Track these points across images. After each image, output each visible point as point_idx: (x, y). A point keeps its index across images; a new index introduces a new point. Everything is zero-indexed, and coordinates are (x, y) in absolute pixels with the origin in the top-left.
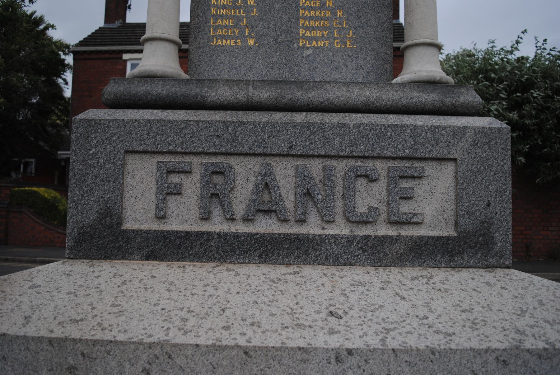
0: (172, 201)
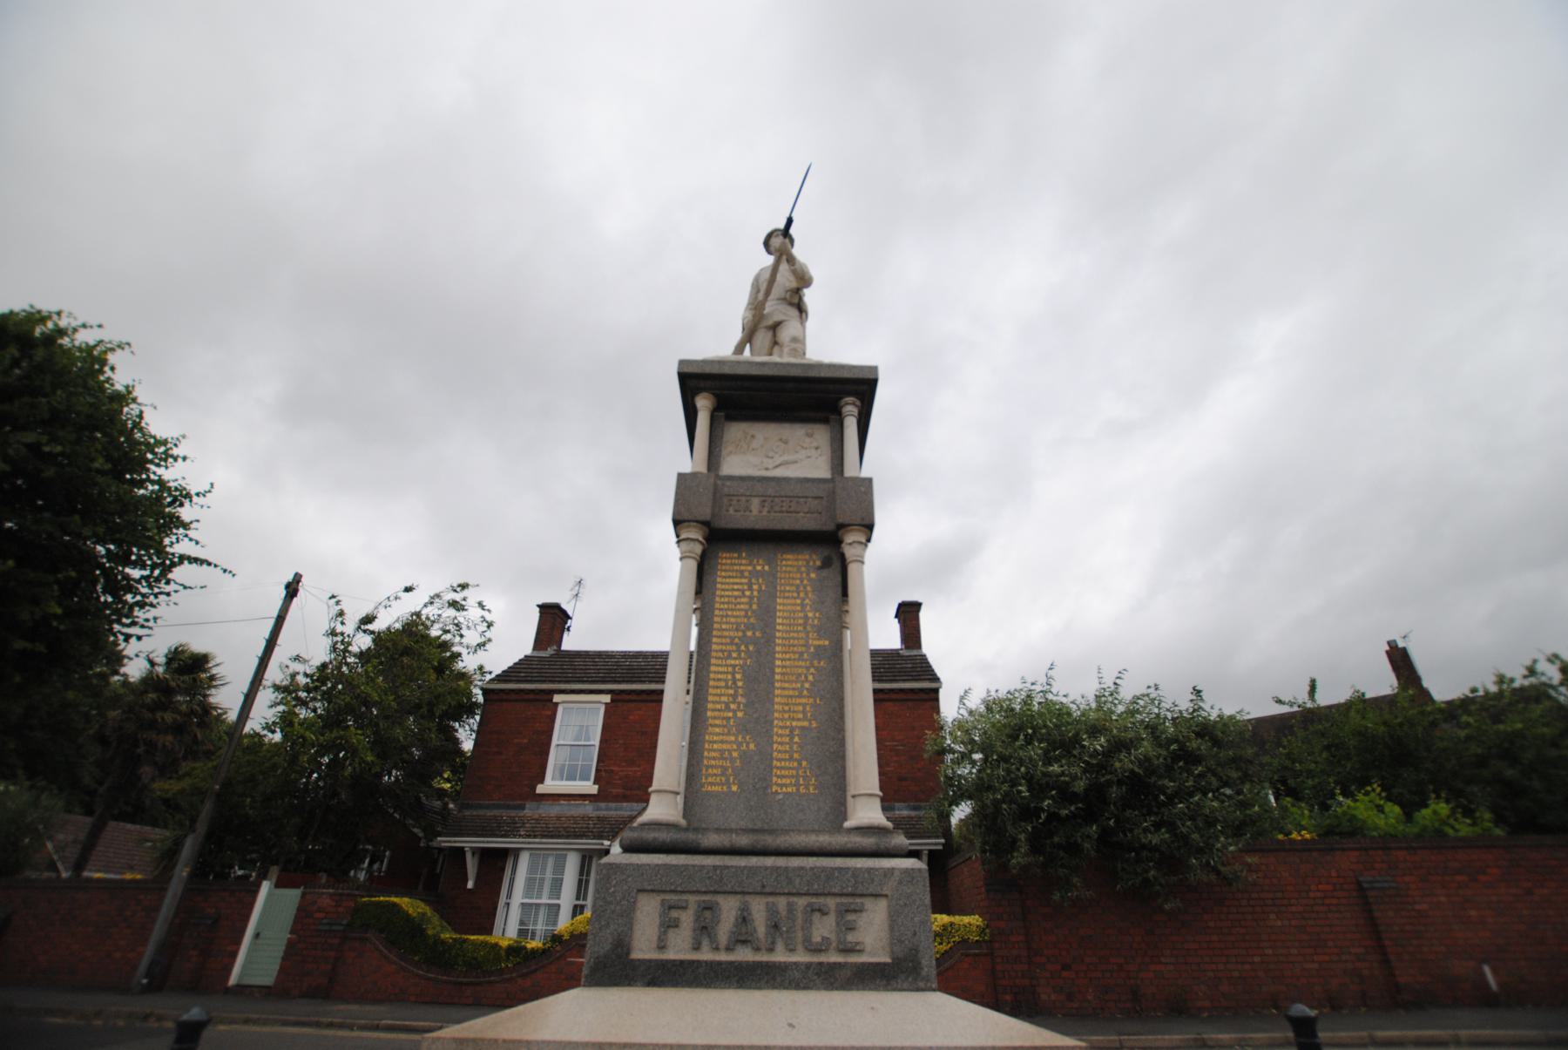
0: (671, 934)
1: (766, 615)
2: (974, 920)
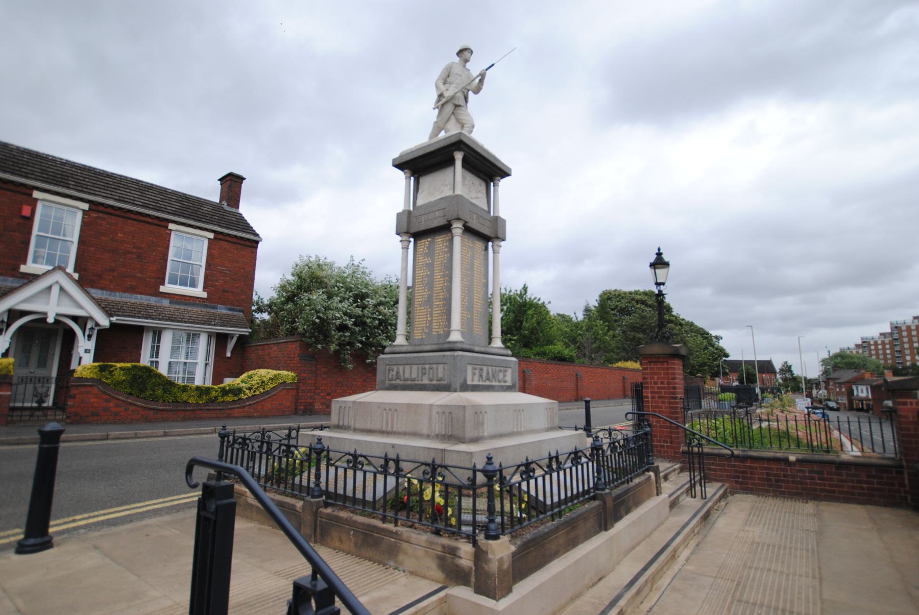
1: (472, 265)
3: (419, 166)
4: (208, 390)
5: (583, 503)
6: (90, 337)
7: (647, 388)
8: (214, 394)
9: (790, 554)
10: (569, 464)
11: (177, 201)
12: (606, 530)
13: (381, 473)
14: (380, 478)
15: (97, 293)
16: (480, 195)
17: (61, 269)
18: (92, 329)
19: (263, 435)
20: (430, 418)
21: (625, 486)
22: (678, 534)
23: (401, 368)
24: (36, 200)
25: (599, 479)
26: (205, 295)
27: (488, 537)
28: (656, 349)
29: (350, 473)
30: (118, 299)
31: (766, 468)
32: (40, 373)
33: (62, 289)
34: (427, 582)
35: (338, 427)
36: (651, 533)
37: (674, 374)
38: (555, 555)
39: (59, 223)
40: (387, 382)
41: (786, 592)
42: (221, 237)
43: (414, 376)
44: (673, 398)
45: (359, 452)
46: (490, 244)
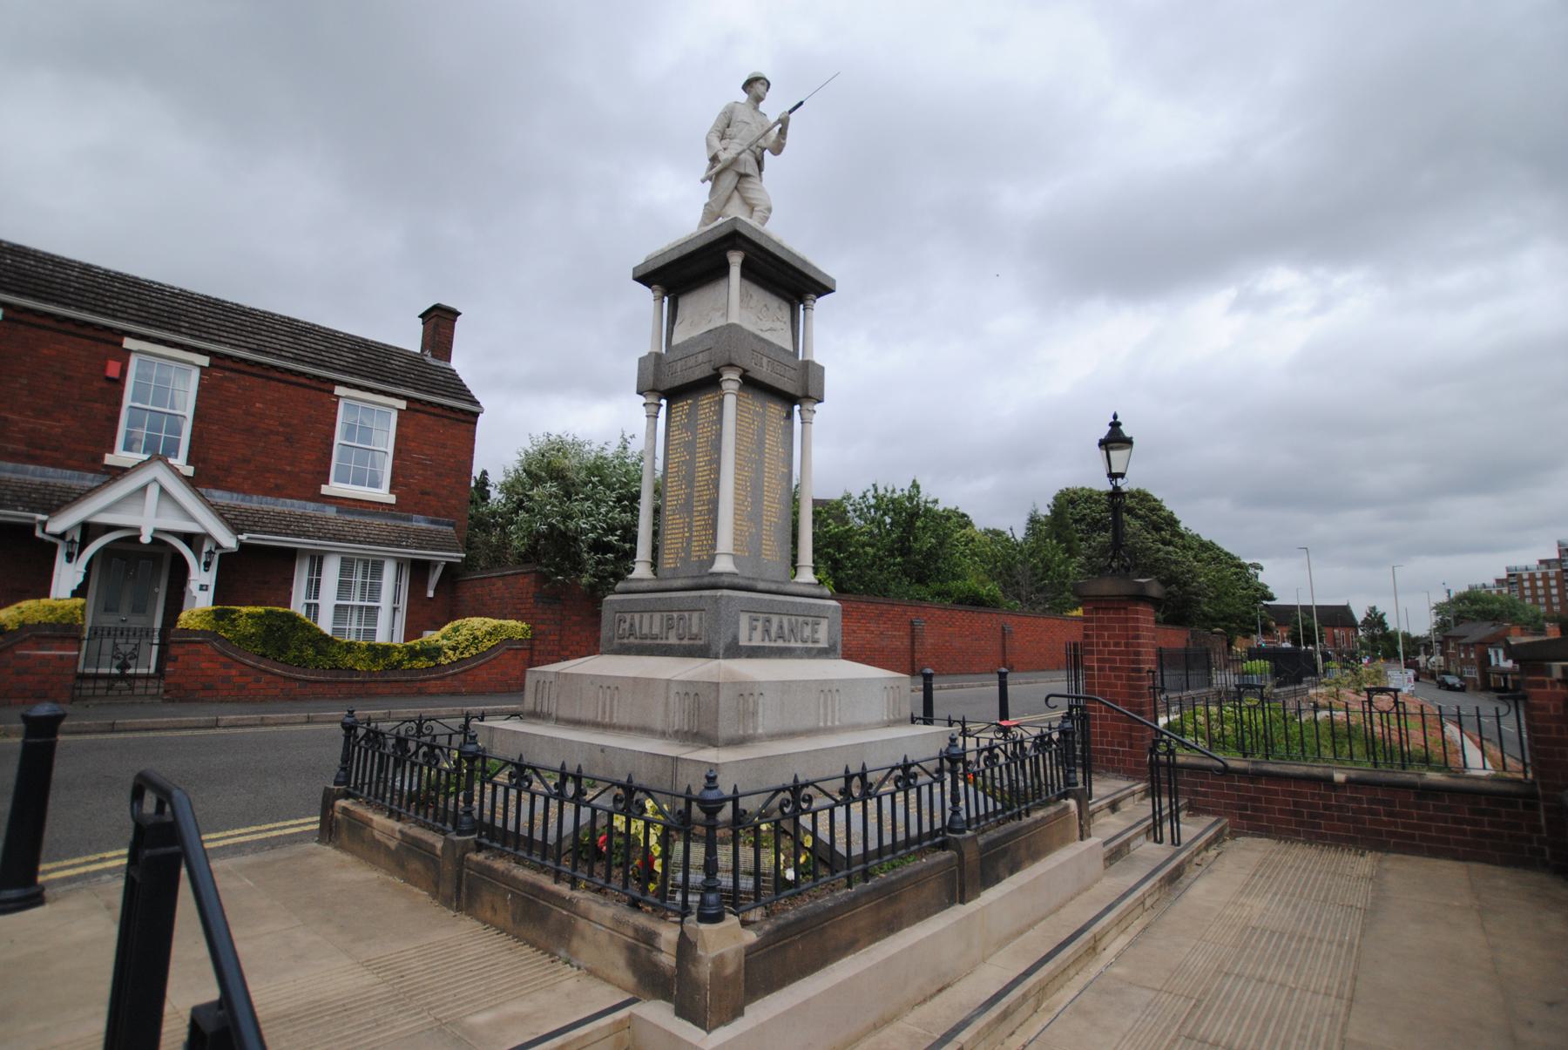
1: (761, 443)
2: (521, 625)
3: (677, 276)
4: (387, 650)
5: (922, 853)
6: (207, 565)
7: (1092, 653)
8: (396, 656)
9: (1307, 950)
10: (889, 787)
11: (352, 351)
12: (962, 902)
13: (556, 796)
14: (554, 803)
15: (221, 497)
16: (778, 325)
17: (163, 459)
18: (210, 553)
19: (420, 726)
20: (667, 704)
21: (1013, 825)
22: (1109, 908)
23: (637, 616)
24: (129, 352)
25: (955, 812)
26: (392, 499)
27: (704, 918)
28: (1107, 587)
29: (513, 793)
30: (255, 506)
31: (1294, 794)
32: (136, 622)
33: (163, 491)
34: (609, 988)
35: (536, 715)
36: (1061, 906)
37: (1137, 628)
38: (850, 946)
39: (164, 386)
40: (616, 641)
41: (1279, 1024)
42: (417, 406)
43: (656, 630)
44: (1134, 670)
45: (526, 760)
46: (797, 408)
